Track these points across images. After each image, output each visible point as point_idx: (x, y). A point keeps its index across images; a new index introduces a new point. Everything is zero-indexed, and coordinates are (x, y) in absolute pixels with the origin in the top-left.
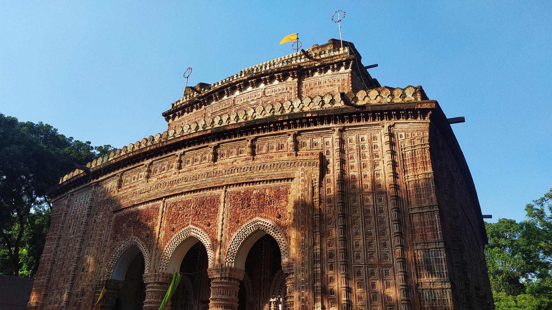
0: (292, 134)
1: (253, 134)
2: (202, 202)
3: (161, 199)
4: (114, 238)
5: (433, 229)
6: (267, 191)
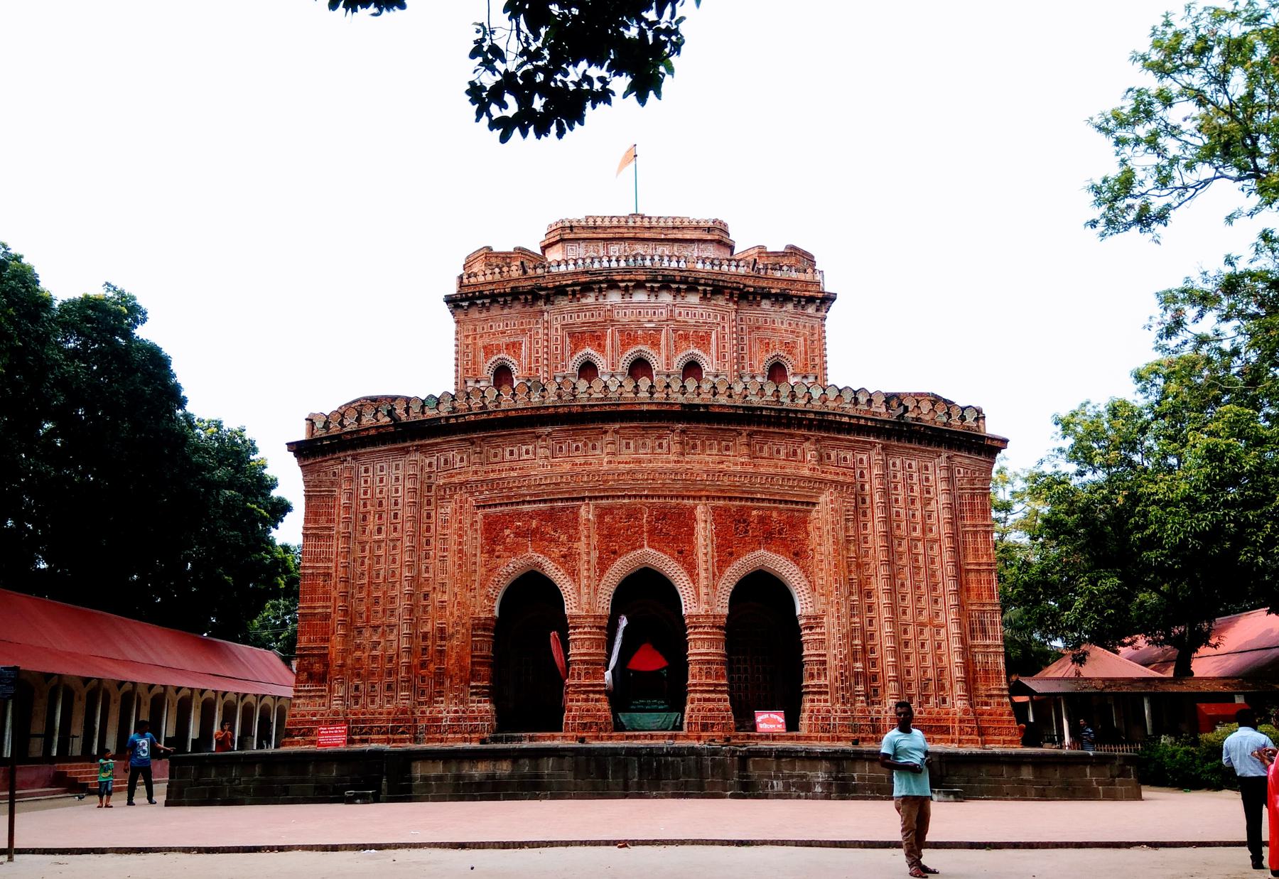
0: (813, 439)
1: (749, 425)
2: (663, 515)
3: (583, 499)
4: (491, 552)
5: (991, 590)
6: (775, 514)
